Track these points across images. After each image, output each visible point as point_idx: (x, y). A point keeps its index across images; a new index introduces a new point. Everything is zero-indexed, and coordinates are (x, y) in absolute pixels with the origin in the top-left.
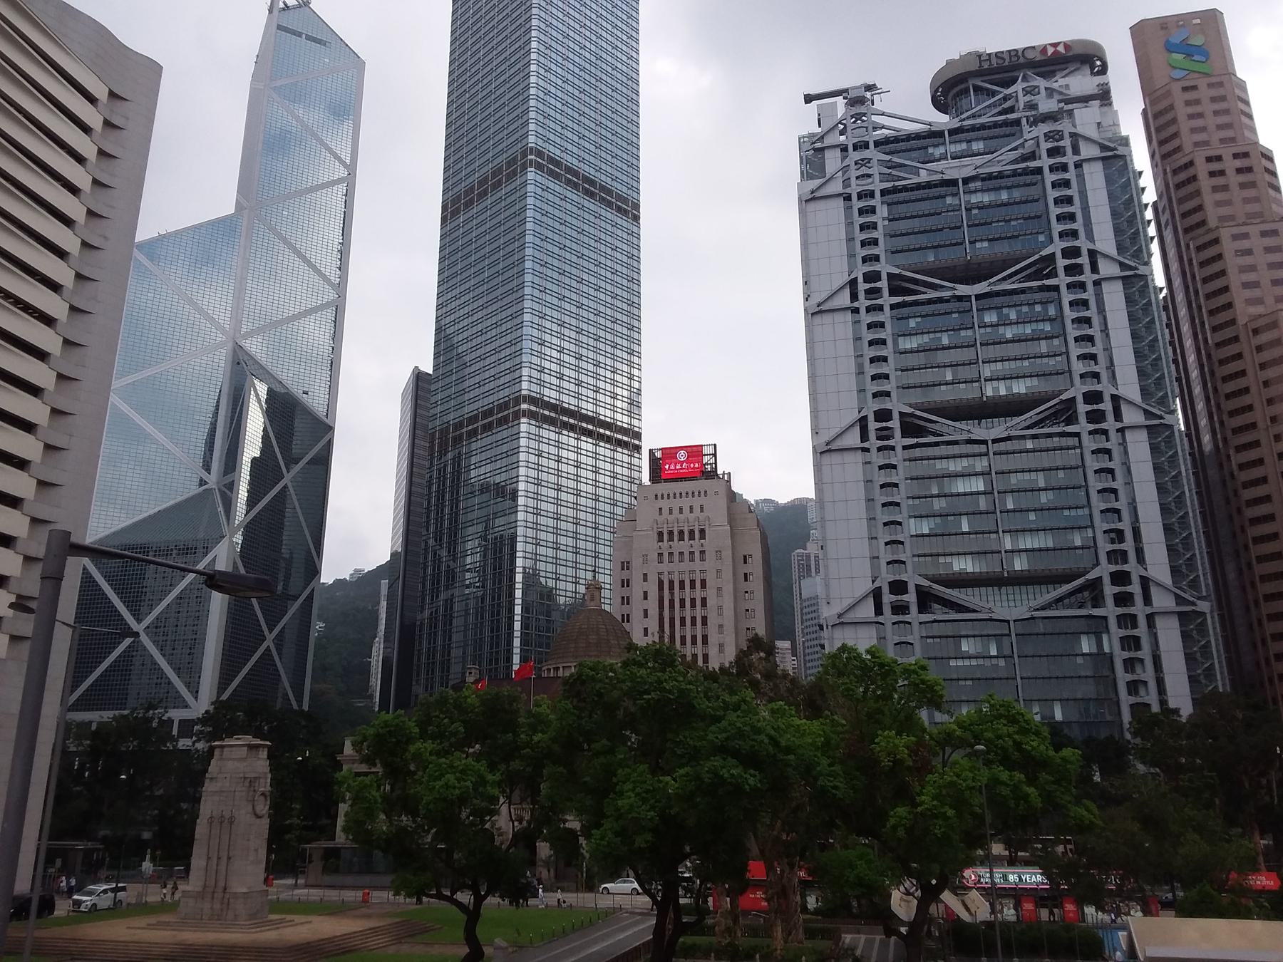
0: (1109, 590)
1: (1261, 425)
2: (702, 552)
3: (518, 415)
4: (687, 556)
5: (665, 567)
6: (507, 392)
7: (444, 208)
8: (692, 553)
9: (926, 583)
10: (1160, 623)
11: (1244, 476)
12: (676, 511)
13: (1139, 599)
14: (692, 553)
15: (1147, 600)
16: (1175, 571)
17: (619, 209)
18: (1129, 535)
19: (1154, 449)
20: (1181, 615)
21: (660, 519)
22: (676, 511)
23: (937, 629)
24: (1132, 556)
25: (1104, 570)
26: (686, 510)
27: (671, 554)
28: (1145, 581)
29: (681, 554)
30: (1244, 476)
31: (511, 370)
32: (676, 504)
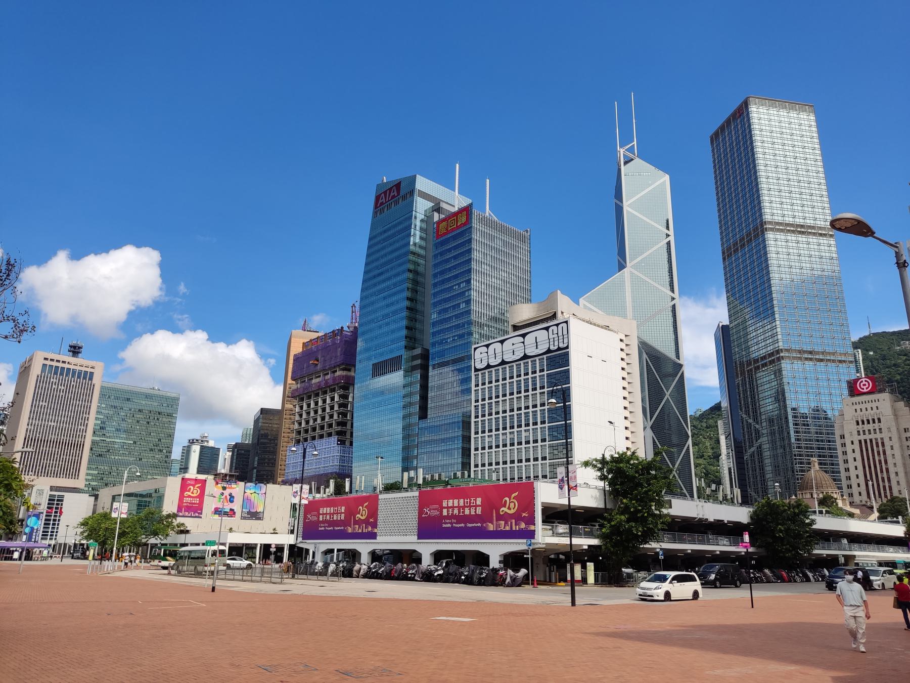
2: (880, 429)
3: (779, 359)
4: (872, 432)
5: (862, 437)
6: (772, 347)
7: (723, 253)
8: (875, 430)
12: (864, 410)
14: (875, 430)
17: (821, 235)
21: (856, 414)
22: (864, 410)
26: (869, 409)
27: (864, 431)
29: (869, 430)
31: (772, 336)
32: (863, 406)
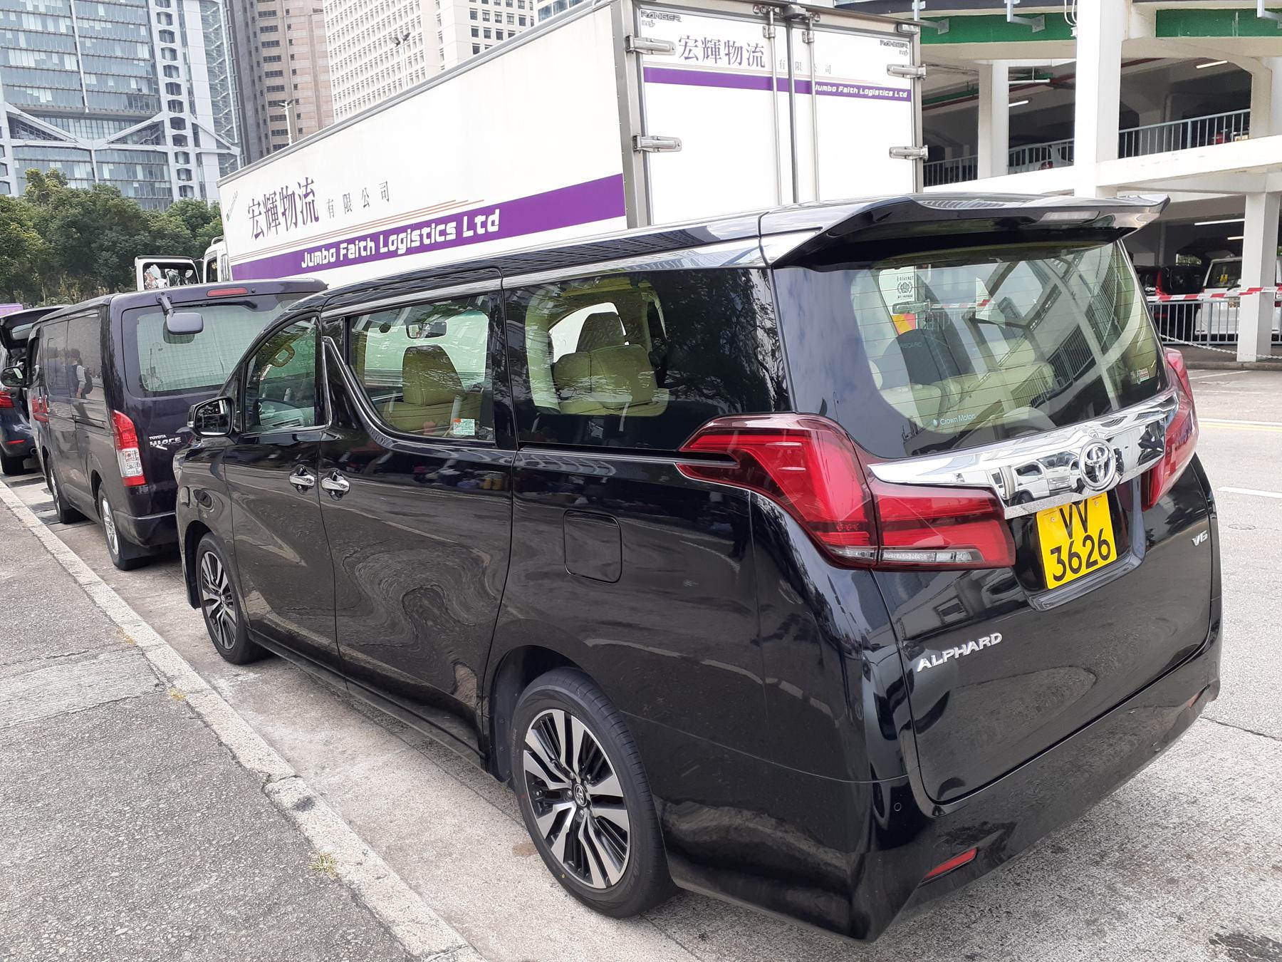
0: (169, 132)
1: (279, 14)
9: (19, 112)
10: (204, 158)
11: (266, 52)
13: (191, 141)
15: (197, 143)
16: (216, 122)
18: (184, 90)
19: (204, 19)
20: (219, 155)
23: (27, 154)
24: (186, 106)
25: (165, 116)
28: (195, 127)
30: (266, 52)
